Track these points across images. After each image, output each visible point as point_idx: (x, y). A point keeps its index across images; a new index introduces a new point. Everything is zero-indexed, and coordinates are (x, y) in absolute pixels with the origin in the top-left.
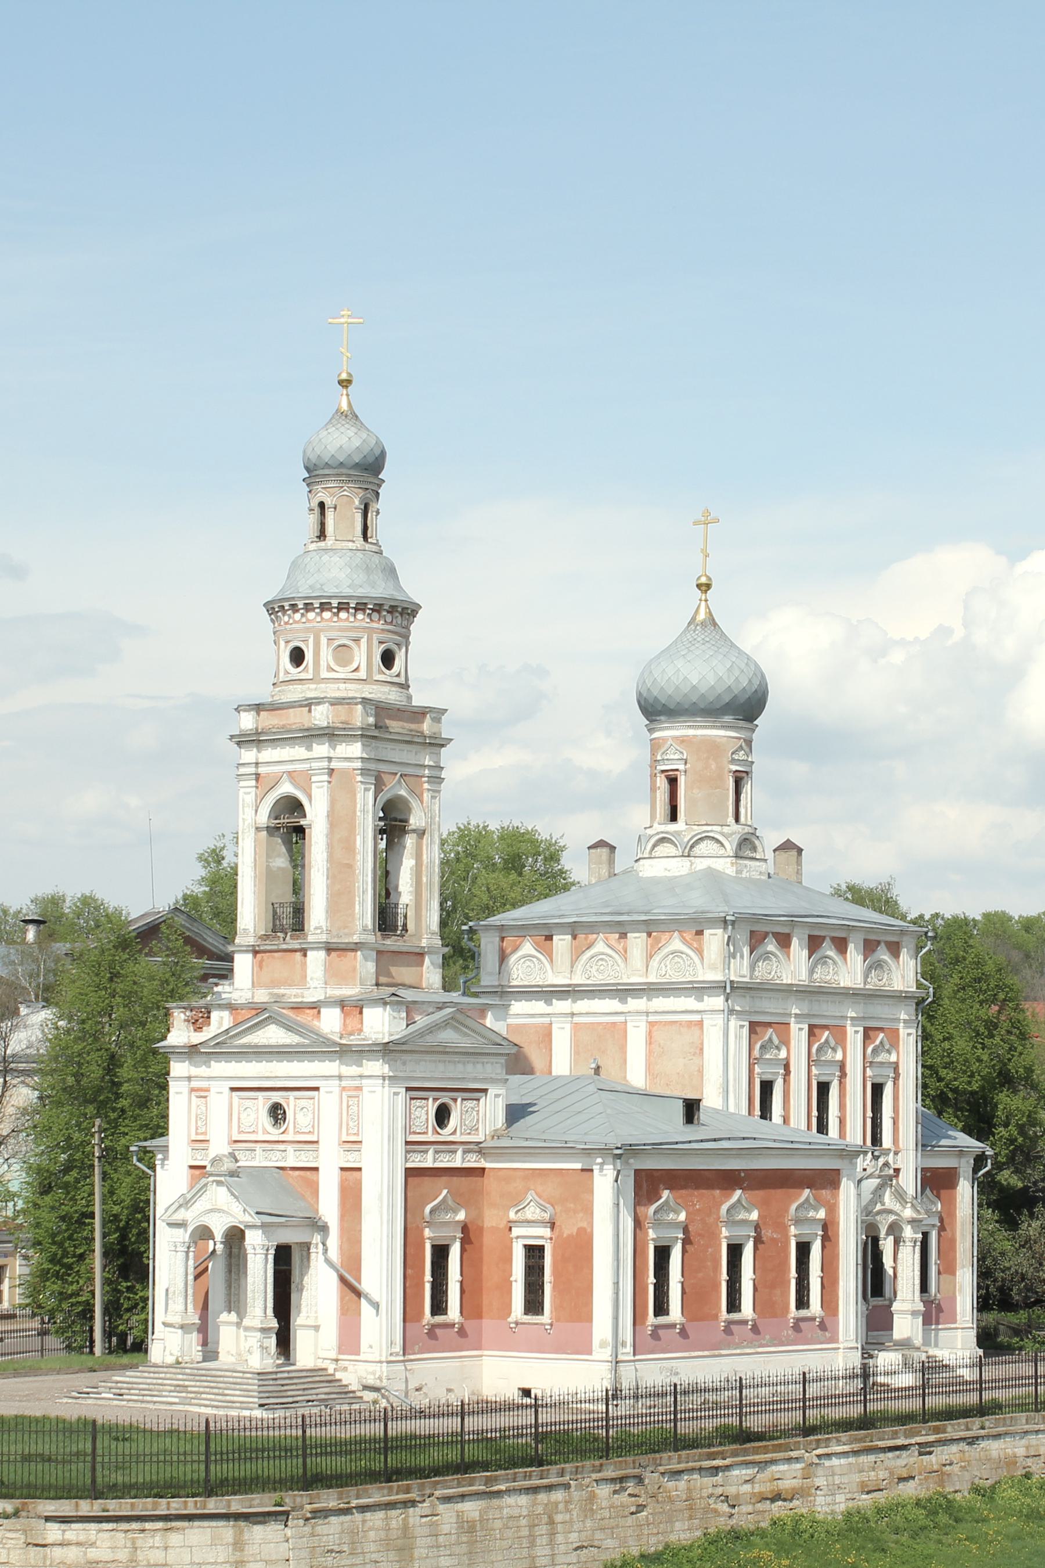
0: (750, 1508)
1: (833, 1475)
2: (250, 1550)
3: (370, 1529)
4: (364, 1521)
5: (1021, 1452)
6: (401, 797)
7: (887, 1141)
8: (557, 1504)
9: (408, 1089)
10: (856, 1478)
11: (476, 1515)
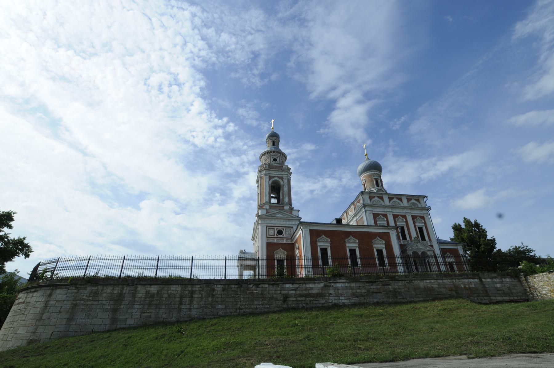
0: (294, 299)
1: (338, 290)
2: (53, 297)
3: (105, 293)
4: (102, 290)
5: (435, 286)
6: (276, 180)
7: (427, 239)
8: (195, 291)
9: (267, 226)
10: (350, 291)
11: (156, 292)
